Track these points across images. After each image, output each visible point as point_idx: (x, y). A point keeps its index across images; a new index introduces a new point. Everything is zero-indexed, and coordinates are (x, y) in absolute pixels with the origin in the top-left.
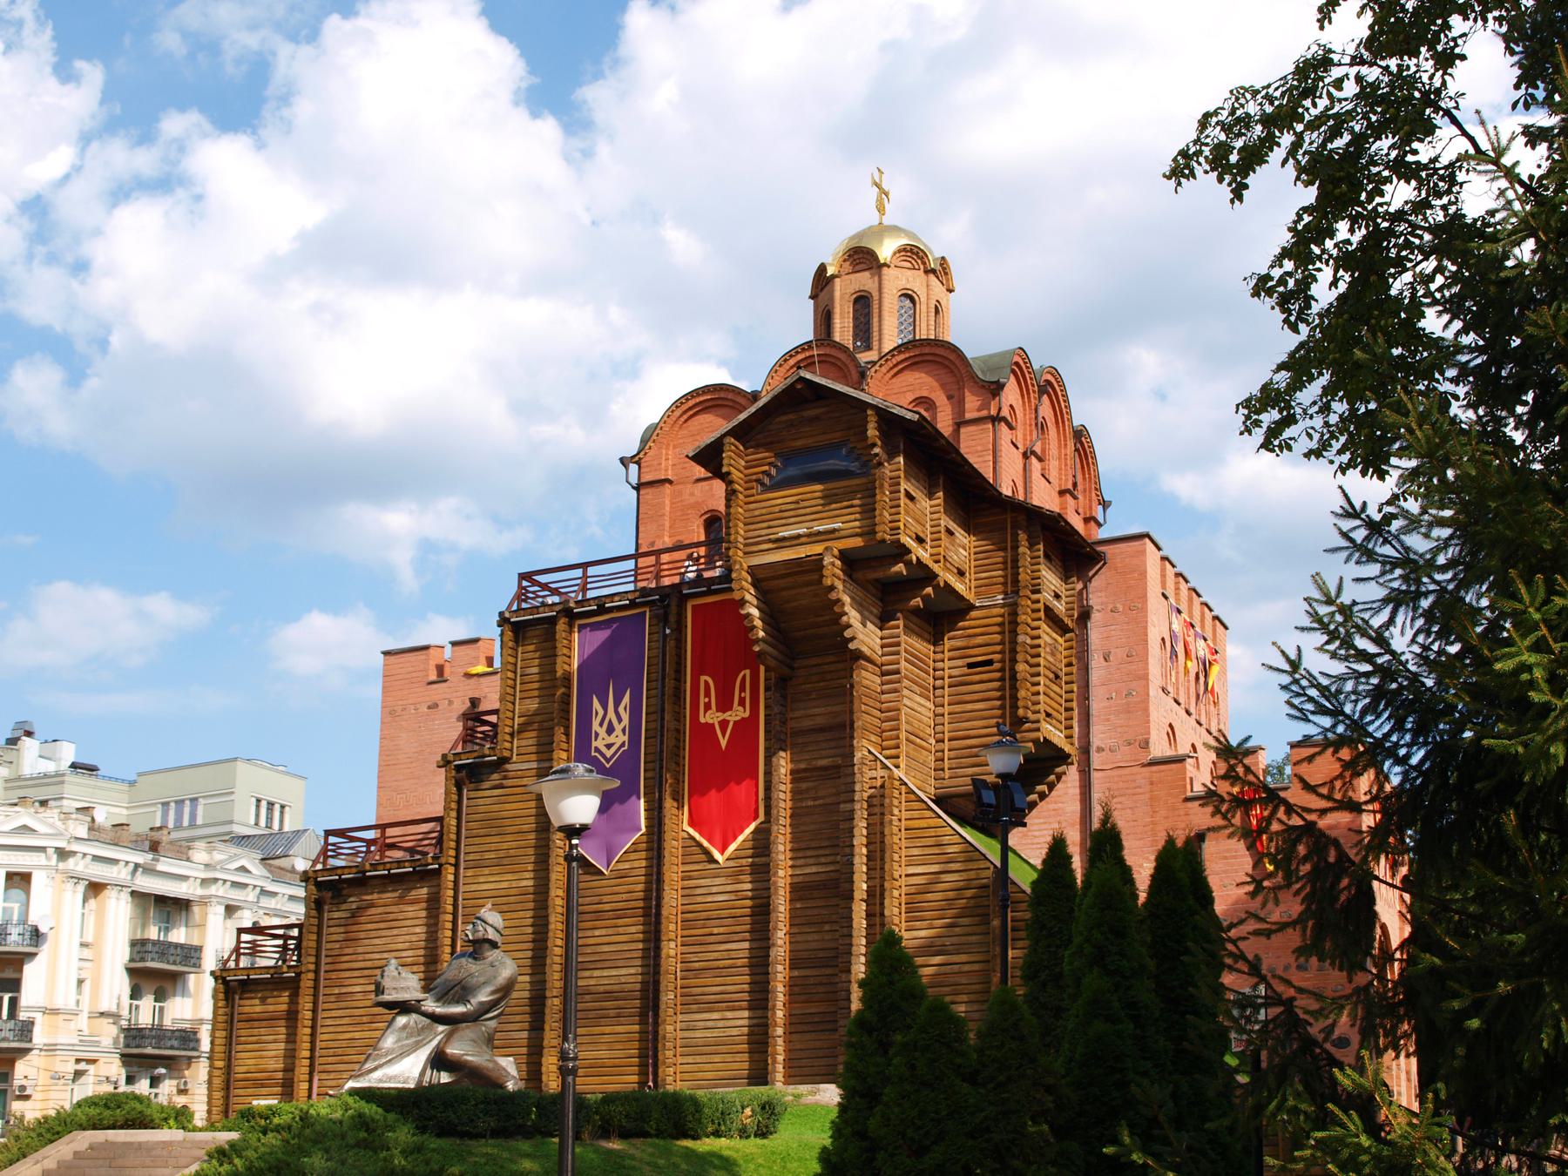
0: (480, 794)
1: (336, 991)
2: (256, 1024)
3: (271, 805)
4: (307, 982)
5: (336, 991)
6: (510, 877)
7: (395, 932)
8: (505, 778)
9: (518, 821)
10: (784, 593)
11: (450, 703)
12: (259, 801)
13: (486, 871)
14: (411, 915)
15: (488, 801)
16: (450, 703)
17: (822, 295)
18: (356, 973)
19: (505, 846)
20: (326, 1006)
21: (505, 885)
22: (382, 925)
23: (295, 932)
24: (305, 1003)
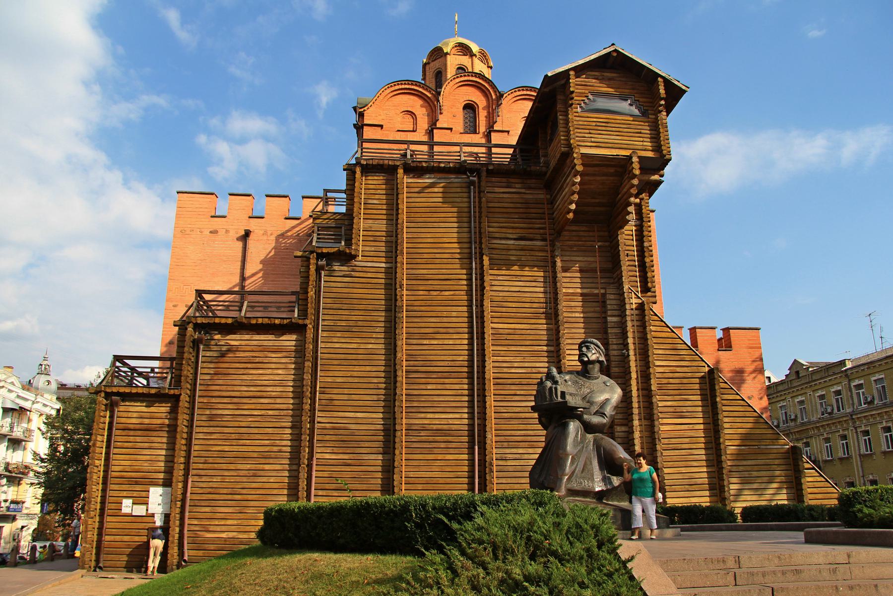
0: (333, 279)
1: (208, 412)
5: (208, 412)
7: (261, 372)
8: (353, 271)
9: (364, 302)
11: (227, 231)
13: (339, 334)
14: (274, 360)
15: (339, 285)
16: (227, 231)
17: (432, 64)
18: (225, 400)
19: (354, 318)
20: (199, 423)
21: (355, 346)
22: (249, 366)
24: (183, 418)
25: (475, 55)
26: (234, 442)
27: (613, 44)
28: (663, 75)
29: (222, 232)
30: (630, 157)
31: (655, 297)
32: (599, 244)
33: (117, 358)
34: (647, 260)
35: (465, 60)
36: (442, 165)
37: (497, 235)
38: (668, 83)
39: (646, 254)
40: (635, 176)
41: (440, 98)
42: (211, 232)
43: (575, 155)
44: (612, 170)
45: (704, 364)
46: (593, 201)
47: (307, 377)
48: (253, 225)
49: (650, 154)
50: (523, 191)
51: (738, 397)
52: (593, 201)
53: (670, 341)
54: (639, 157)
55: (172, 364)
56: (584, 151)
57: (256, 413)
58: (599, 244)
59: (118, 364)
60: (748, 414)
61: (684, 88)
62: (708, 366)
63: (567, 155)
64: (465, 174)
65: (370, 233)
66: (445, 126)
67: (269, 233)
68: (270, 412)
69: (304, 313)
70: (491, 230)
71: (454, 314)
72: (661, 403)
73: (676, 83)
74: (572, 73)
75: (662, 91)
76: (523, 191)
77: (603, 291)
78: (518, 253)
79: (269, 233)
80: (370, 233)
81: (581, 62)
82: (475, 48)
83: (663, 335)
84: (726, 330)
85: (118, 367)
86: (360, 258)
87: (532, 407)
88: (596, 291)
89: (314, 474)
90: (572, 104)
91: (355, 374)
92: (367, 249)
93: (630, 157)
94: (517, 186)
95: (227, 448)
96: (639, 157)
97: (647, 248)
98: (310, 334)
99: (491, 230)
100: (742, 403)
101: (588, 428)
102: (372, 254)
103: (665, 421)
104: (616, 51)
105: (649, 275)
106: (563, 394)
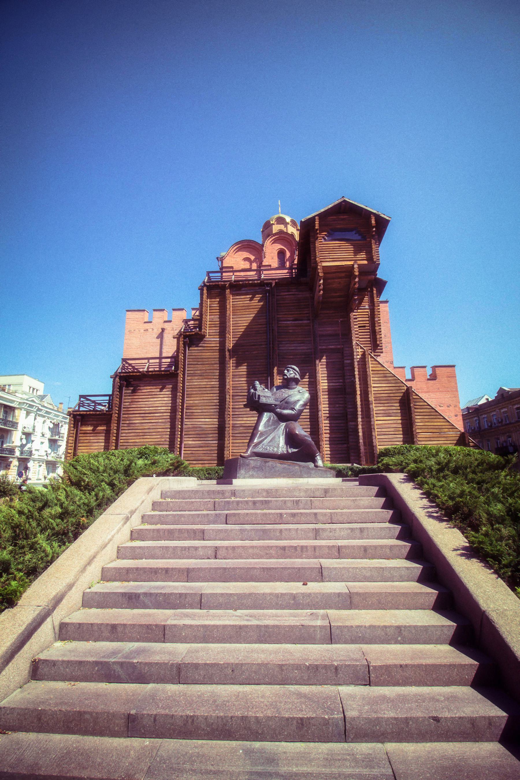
1: (128, 422)
2: (88, 435)
3: (34, 389)
4: (115, 416)
5: (128, 422)
6: (207, 380)
7: (155, 399)
10: (329, 281)
12: (30, 387)
13: (196, 378)
15: (196, 351)
18: (137, 415)
20: (123, 428)
21: (205, 383)
22: (149, 397)
23: (107, 398)
24: (114, 426)
25: (288, 224)
26: (142, 437)
27: (343, 197)
28: (375, 212)
29: (150, 330)
30: (353, 265)
31: (382, 349)
32: (341, 320)
33: (81, 396)
34: (377, 328)
35: (282, 227)
36: (251, 282)
37: (282, 319)
38: (378, 218)
39: (376, 325)
40: (355, 276)
41: (264, 249)
42: (144, 330)
43: (319, 267)
44: (343, 275)
45: (403, 385)
46: (336, 294)
47: (179, 401)
48: (166, 326)
49: (365, 262)
50: (297, 293)
51: (426, 404)
52: (336, 294)
53: (382, 372)
54: (358, 265)
55: (110, 398)
56: (324, 264)
57: (153, 421)
58: (341, 320)
59: (82, 399)
60: (432, 414)
61: (387, 218)
62: (406, 386)
63: (316, 268)
64: (264, 286)
65: (213, 323)
66: (267, 264)
67: (175, 329)
68: (160, 421)
69: (177, 368)
70: (278, 316)
71: (258, 364)
72: (375, 408)
73: (383, 216)
74: (316, 218)
75: (373, 222)
76: (297, 293)
77: (342, 346)
78: (294, 328)
79: (175, 329)
80: (213, 323)
81: (322, 210)
82: (288, 219)
83: (377, 369)
84: (434, 368)
85: (82, 401)
86: (207, 336)
87: (244, 405)
88: (339, 347)
89: (183, 452)
90: (318, 237)
91: (204, 398)
92: (211, 331)
93: (353, 265)
94: (293, 290)
95: (137, 441)
96: (358, 265)
97: (377, 321)
98: (180, 379)
99: (278, 316)
100: (428, 407)
101: (282, 418)
102: (214, 334)
103: (379, 418)
104: (345, 201)
105: (378, 337)
106: (259, 396)
